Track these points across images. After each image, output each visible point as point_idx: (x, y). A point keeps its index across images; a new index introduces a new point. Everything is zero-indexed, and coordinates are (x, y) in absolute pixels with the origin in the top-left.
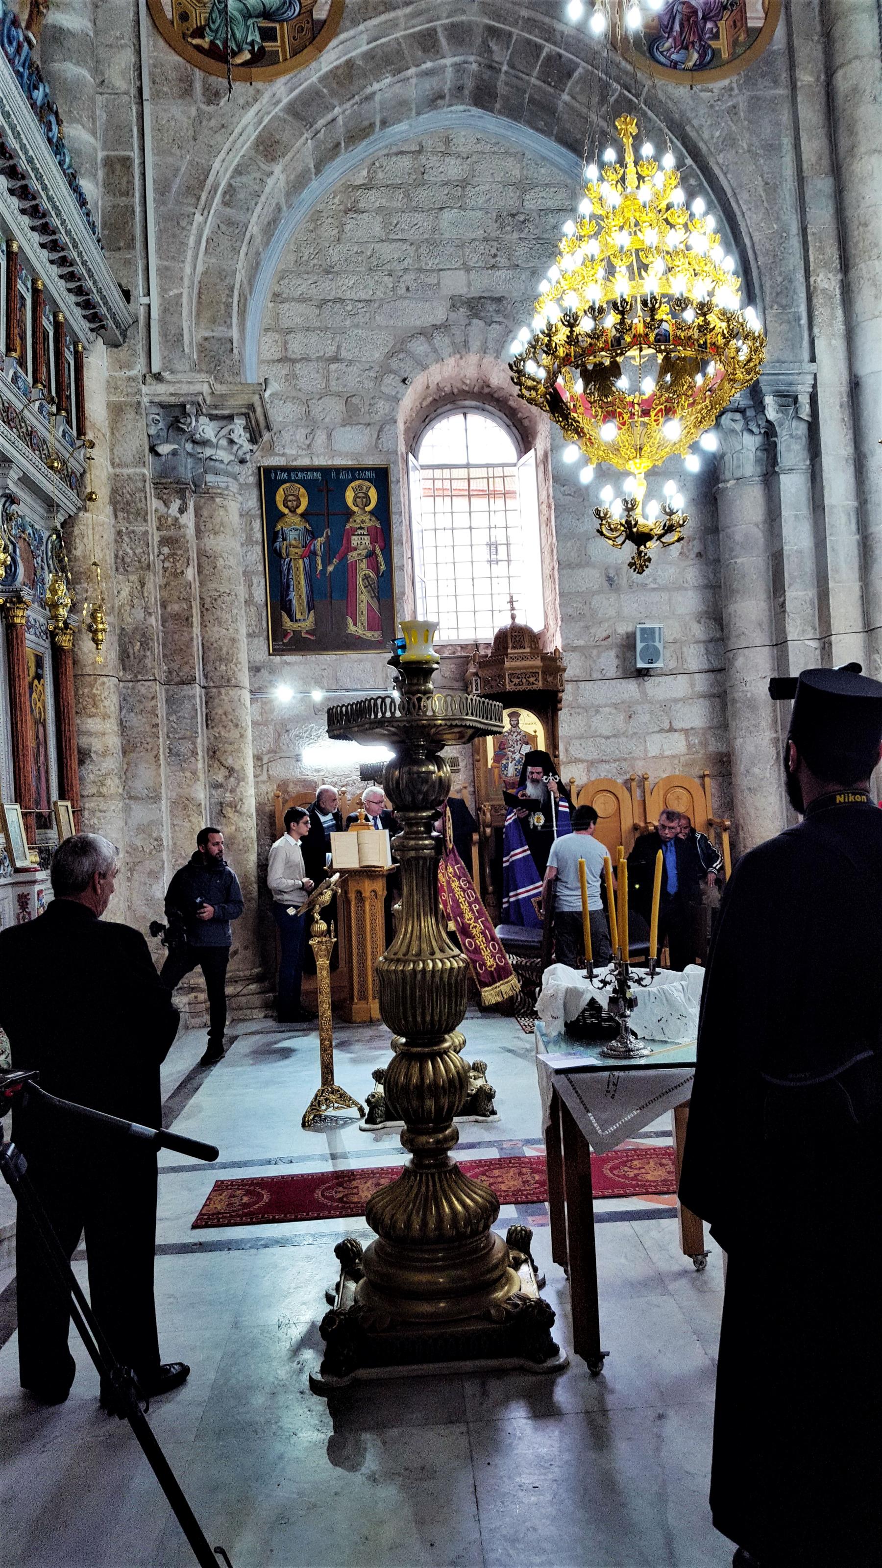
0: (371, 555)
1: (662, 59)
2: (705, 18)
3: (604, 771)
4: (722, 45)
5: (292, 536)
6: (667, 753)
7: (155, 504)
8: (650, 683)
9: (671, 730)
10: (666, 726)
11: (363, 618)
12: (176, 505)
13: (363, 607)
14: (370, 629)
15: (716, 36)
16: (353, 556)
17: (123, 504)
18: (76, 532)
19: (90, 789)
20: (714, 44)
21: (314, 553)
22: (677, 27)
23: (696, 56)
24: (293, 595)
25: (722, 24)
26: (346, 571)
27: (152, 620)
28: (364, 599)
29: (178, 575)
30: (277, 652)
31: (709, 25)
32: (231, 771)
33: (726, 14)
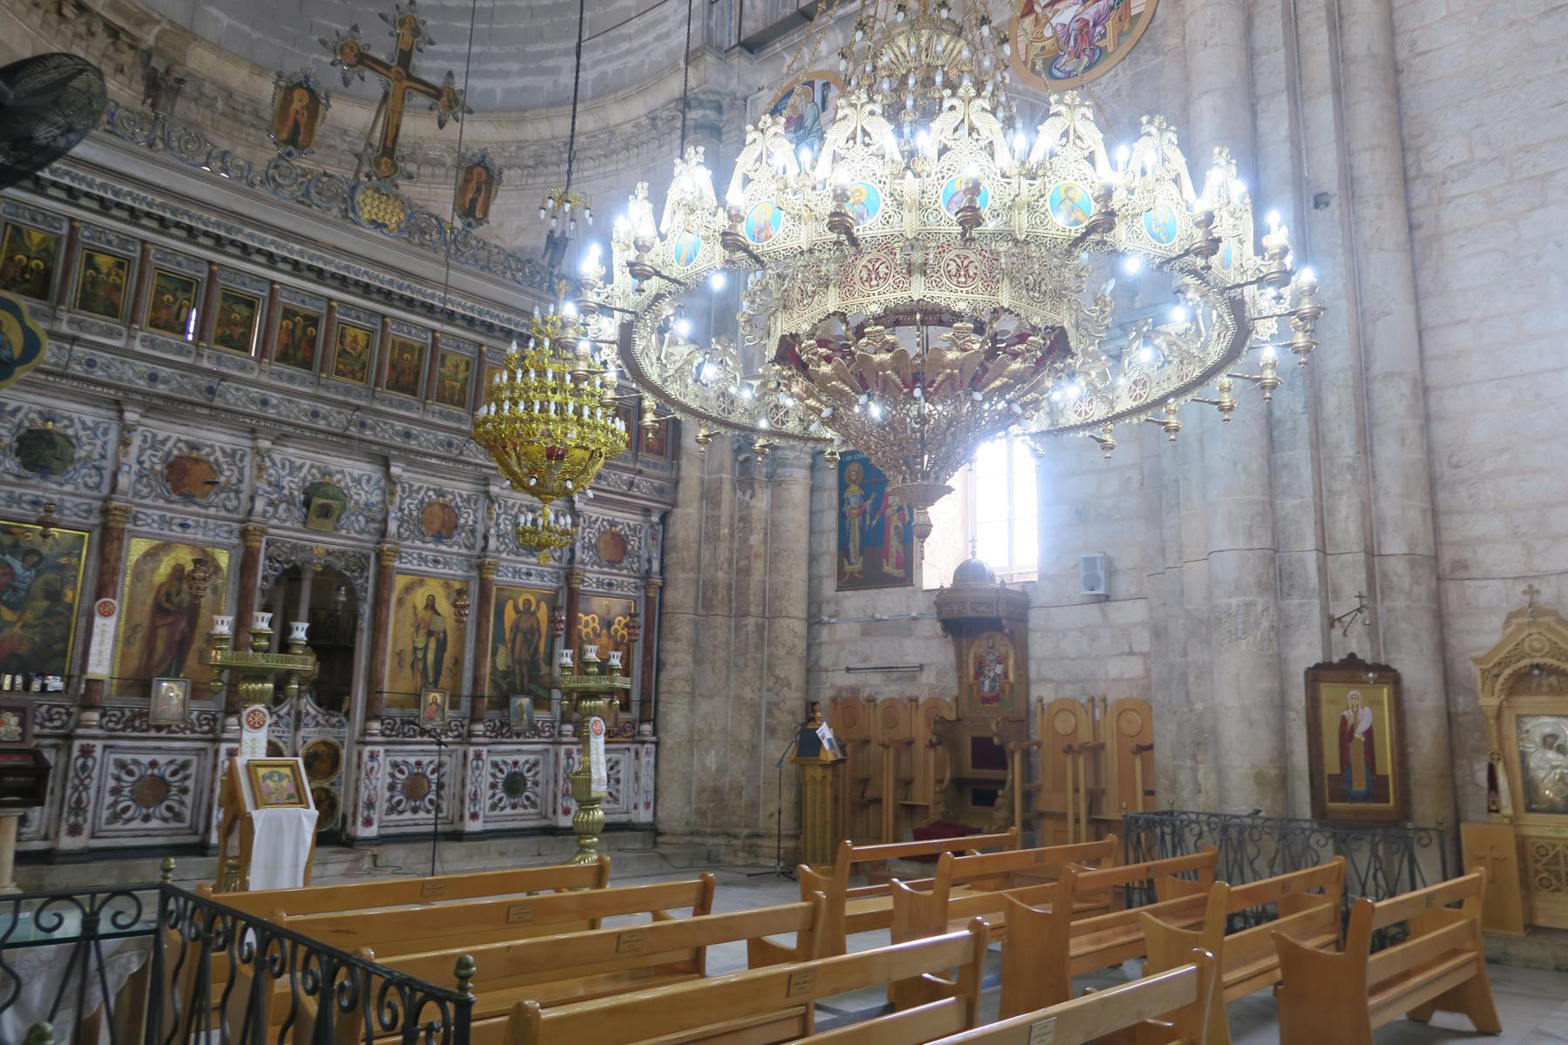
0: (900, 509)
1: (1059, 74)
2: (1095, 25)
3: (1068, 692)
4: (1108, 43)
5: (852, 500)
6: (1126, 676)
7: (739, 493)
8: (1111, 607)
9: (1131, 653)
10: (1126, 649)
11: (893, 560)
12: (749, 493)
13: (893, 550)
14: (898, 567)
15: (1103, 36)
16: (889, 511)
17: (710, 496)
19: (663, 688)
20: (1101, 44)
21: (864, 512)
22: (1072, 43)
23: (1086, 59)
24: (851, 546)
25: (1109, 24)
26: (884, 523)
27: (721, 575)
28: (894, 544)
29: (745, 540)
30: (839, 589)
31: (1098, 29)
32: (777, 678)
33: (1113, 14)
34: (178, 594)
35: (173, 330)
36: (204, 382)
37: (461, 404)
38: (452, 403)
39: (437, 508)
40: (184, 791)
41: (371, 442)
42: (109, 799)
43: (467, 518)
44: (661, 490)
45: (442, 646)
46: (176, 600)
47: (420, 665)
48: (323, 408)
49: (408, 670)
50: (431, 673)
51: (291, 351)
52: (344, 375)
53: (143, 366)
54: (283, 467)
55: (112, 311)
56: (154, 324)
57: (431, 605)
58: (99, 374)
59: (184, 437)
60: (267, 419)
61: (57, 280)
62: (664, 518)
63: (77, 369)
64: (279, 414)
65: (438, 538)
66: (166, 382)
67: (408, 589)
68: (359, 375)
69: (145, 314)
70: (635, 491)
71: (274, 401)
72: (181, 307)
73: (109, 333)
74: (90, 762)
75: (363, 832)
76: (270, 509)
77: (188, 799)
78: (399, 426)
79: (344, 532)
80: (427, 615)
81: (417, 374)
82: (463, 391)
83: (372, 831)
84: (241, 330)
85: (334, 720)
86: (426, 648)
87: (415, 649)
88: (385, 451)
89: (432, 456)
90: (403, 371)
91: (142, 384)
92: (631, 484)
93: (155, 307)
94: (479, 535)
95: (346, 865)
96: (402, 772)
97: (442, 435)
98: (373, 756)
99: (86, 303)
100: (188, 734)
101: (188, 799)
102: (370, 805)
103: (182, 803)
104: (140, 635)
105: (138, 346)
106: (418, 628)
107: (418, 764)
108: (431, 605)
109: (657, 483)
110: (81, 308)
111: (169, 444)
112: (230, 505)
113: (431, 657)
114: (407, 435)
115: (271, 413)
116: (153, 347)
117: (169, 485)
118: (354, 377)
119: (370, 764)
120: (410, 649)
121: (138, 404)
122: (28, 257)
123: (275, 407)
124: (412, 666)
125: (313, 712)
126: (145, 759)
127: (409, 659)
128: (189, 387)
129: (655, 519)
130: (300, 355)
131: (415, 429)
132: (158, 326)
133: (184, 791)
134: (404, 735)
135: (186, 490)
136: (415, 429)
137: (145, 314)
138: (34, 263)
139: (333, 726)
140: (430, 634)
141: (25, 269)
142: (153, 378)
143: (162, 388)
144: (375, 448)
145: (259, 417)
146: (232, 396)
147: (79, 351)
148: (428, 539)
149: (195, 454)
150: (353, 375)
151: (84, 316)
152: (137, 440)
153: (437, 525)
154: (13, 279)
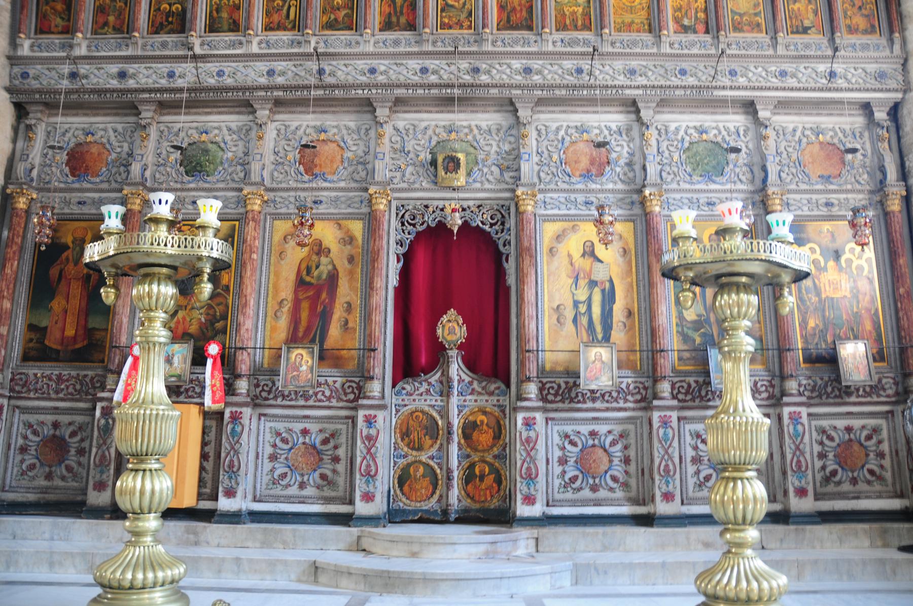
18: (905, 111)
34: (317, 267)
35: (285, 29)
36: (313, 66)
37: (587, 27)
38: (576, 28)
39: (581, 146)
40: (336, 459)
41: (487, 86)
42: (268, 466)
43: (621, 150)
44: (881, 76)
45: (609, 297)
46: (316, 273)
47: (584, 320)
48: (431, 64)
49: (569, 326)
50: (599, 328)
51: (394, 19)
52: (450, 27)
53: (263, 66)
54: (407, 130)
55: (235, 27)
56: (268, 28)
57: (589, 252)
58: (229, 81)
59: (313, 123)
60: (376, 86)
61: (188, 15)
62: (895, 111)
63: (212, 82)
64: (389, 78)
65: (587, 175)
66: (283, 74)
67: (559, 238)
68: (466, 24)
69: (258, 19)
70: (841, 83)
71: (383, 68)
72: (289, 7)
73: (233, 45)
74: (238, 429)
75: (523, 510)
76: (398, 174)
77: (341, 467)
78: (517, 64)
79: (478, 185)
80: (587, 263)
81: (530, 9)
82: (587, 15)
83: (536, 510)
84: (343, 13)
85: (492, 387)
86: (590, 299)
87: (576, 304)
88: (506, 93)
89: (559, 87)
90: (514, 9)
91: (263, 81)
92: (832, 74)
93: (268, 14)
94: (637, 168)
95: (482, 548)
96: (574, 444)
97: (568, 64)
98: (529, 423)
99: (213, 27)
100: (334, 403)
101: (341, 467)
102: (531, 477)
103: (334, 471)
104: (285, 309)
105: (255, 49)
106: (577, 278)
107: (593, 434)
108: (589, 252)
109: (872, 67)
110: (210, 31)
111: (300, 132)
112: (357, 177)
113: (596, 310)
114: (528, 71)
115: (381, 79)
116: (269, 47)
117: (301, 168)
118: (461, 27)
119: (525, 435)
120: (570, 303)
121: (265, 99)
122: (170, 5)
123: (385, 73)
124: (575, 321)
125: (467, 379)
126: (298, 427)
127: (569, 314)
128: (303, 74)
129: (881, 115)
130: (403, 20)
131: (536, 64)
132: (272, 29)
133: (336, 459)
134: (572, 401)
135: (316, 171)
136: (536, 64)
137: (258, 19)
138: (174, 8)
139: (491, 394)
140: (593, 284)
141: (169, 14)
142: (271, 73)
143: (280, 80)
144: (494, 91)
145: (368, 86)
146: (342, 72)
147: (212, 67)
148: (573, 180)
149: (323, 136)
150: (460, 25)
151: (214, 37)
152: (270, 132)
153: (584, 163)
154: (161, 24)
